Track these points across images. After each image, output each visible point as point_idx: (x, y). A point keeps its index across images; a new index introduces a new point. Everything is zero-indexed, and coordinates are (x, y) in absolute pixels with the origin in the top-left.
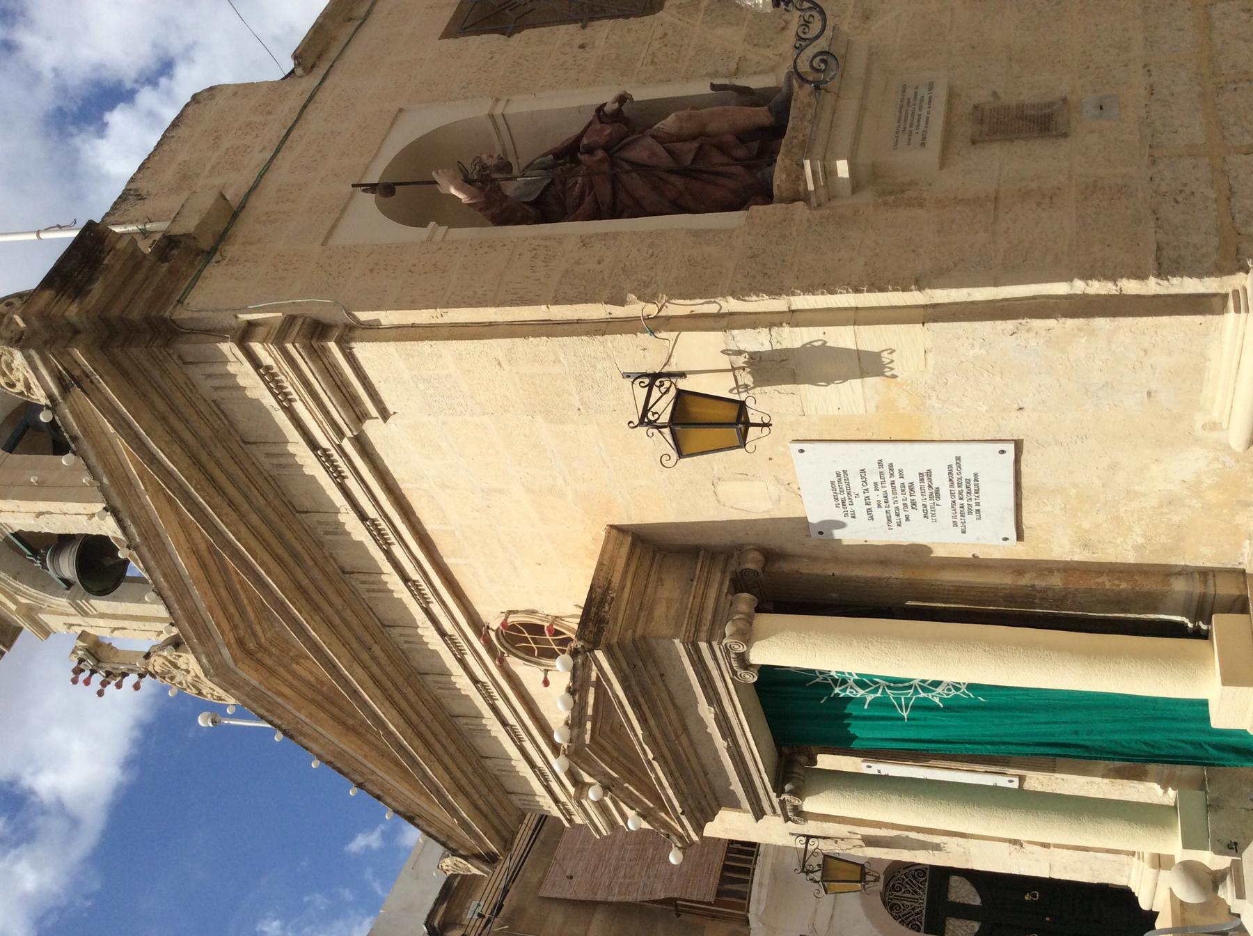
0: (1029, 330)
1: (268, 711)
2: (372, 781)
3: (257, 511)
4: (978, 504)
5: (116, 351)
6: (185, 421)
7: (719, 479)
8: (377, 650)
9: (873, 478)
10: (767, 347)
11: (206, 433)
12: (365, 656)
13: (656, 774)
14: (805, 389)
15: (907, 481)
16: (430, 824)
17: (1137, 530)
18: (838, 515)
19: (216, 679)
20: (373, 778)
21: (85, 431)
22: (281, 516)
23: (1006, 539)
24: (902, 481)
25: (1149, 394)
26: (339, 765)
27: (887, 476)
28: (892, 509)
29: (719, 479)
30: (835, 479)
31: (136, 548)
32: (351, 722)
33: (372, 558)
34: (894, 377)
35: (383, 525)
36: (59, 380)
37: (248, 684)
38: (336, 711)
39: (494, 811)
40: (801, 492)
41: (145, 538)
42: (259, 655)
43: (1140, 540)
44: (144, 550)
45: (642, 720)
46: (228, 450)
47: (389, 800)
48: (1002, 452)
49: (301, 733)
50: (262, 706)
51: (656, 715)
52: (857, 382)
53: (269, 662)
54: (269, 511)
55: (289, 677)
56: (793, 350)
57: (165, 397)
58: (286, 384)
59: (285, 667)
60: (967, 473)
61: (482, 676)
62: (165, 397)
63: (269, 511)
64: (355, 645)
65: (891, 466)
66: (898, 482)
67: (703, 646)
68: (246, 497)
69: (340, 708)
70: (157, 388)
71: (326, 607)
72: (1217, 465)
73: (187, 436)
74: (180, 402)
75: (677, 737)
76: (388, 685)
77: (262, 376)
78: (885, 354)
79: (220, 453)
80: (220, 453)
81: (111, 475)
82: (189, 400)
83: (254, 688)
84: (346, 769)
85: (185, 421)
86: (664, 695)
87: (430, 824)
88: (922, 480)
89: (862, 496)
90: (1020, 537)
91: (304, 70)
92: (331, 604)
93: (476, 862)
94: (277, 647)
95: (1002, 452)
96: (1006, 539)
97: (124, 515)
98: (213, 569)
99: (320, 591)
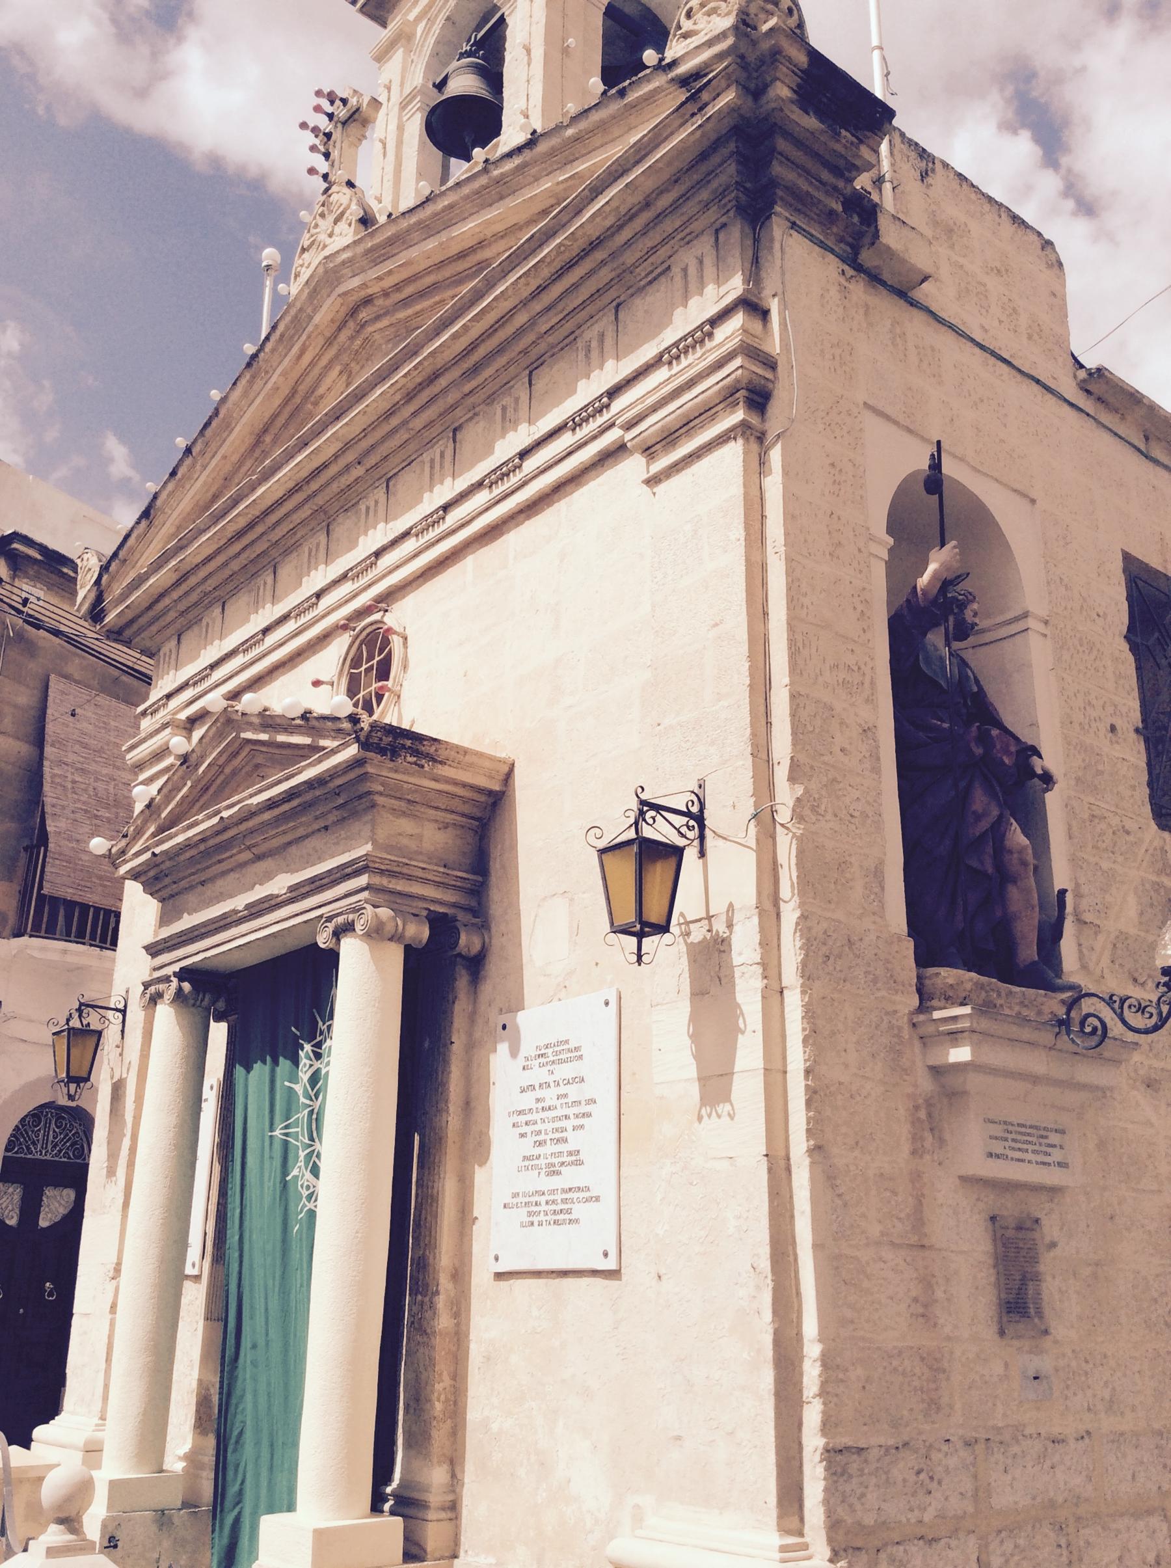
0: (758, 1287)
1: (282, 336)
2: (193, 465)
3: (532, 322)
4: (540, 1224)
5: (732, 146)
6: (644, 232)
7: (572, 900)
8: (359, 471)
9: (573, 1092)
10: (737, 959)
11: (629, 258)
12: (350, 457)
13: (203, 821)
14: (684, 1008)
15: (569, 1134)
16: (140, 538)
18: (528, 1047)
19: (321, 270)
20: (198, 467)
21: (632, 106)
22: (525, 352)
23: (497, 1259)
24: (570, 1128)
25: (679, 1438)
26: (214, 424)
27: (576, 1110)
29: (572, 900)
30: (572, 1045)
31: (485, 170)
32: (268, 439)
33: (472, 465)
34: (700, 1118)
35: (514, 479)
36: (696, 75)
37: (315, 311)
38: (281, 420)
39: (156, 619)
42: (351, 324)
43: (495, 1427)
44: (483, 180)
45: (271, 804)
46: (609, 286)
47: (170, 487)
48: (606, 1255)
49: (253, 377)
50: (287, 328)
51: (278, 821)
52: (692, 1072)
55: (324, 361)
57: (675, 207)
58: (691, 358)
59: (337, 356)
60: (579, 1210)
62: (675, 207)
63: (529, 338)
64: (365, 444)
65: (589, 1115)
66: (568, 1124)
67: (363, 880)
68: (548, 309)
69: (285, 425)
70: (685, 197)
73: (626, 234)
74: (669, 225)
75: (249, 848)
76: (314, 486)
77: (700, 327)
78: (728, 1107)
79: (605, 275)
80: (605, 275)
81: (577, 139)
82: (670, 237)
83: (311, 318)
84: (209, 432)
85: (644, 232)
86: (301, 832)
87: (140, 538)
88: (570, 1154)
89: (550, 1079)
90: (499, 1276)
91: (1084, 381)
92: (415, 414)
93: (93, 595)
94: (362, 347)
95: (606, 1255)
96: (497, 1259)
97: (527, 155)
98: (461, 266)
99: (432, 400)
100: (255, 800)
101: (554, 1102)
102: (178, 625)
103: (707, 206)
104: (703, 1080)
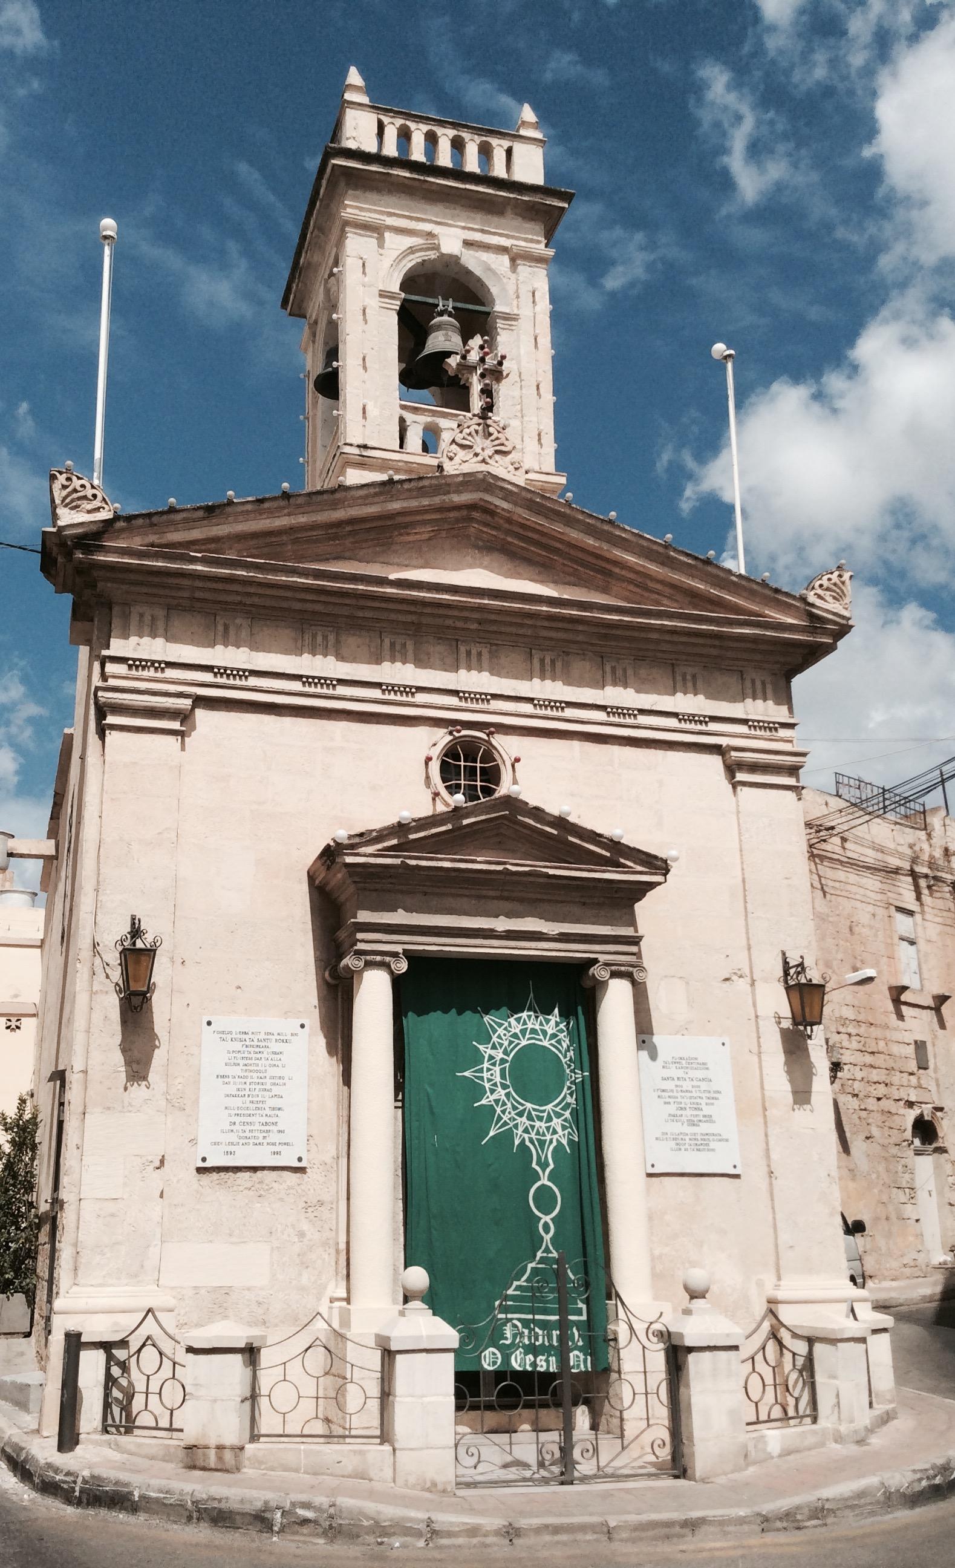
2: (284, 508)
3: (658, 642)
9: (704, 1086)
11: (729, 654)
12: (476, 615)
14: (781, 1058)
15: (703, 1106)
19: (481, 476)
20: (286, 511)
22: (640, 650)
23: (653, 1166)
26: (325, 497)
28: (675, 1094)
29: (687, 983)
32: (348, 528)
33: (580, 685)
35: (629, 721)
37: (458, 492)
40: (679, 1036)
41: (669, 557)
42: (464, 513)
44: (661, 550)
45: (554, 876)
46: (708, 656)
48: (735, 1167)
49: (380, 494)
50: (431, 486)
52: (788, 1087)
53: (452, 515)
54: (651, 647)
55: (428, 517)
56: (808, 1056)
58: (762, 733)
60: (712, 1145)
61: (420, 698)
63: (651, 647)
64: (493, 617)
65: (716, 1099)
66: (703, 1102)
71: (546, 624)
73: (735, 645)
74: (758, 657)
76: (428, 610)
79: (714, 652)
80: (714, 652)
81: (733, 582)
82: (752, 661)
83: (449, 493)
84: (314, 497)
87: (186, 520)
88: (705, 1116)
89: (686, 1076)
90: (650, 1175)
92: (545, 628)
93: (94, 528)
94: (459, 529)
95: (735, 1167)
97: (700, 565)
98: (591, 559)
99: (566, 630)
100: (551, 872)
101: (690, 1088)
102: (175, 602)
103: (777, 663)
104: (795, 1093)
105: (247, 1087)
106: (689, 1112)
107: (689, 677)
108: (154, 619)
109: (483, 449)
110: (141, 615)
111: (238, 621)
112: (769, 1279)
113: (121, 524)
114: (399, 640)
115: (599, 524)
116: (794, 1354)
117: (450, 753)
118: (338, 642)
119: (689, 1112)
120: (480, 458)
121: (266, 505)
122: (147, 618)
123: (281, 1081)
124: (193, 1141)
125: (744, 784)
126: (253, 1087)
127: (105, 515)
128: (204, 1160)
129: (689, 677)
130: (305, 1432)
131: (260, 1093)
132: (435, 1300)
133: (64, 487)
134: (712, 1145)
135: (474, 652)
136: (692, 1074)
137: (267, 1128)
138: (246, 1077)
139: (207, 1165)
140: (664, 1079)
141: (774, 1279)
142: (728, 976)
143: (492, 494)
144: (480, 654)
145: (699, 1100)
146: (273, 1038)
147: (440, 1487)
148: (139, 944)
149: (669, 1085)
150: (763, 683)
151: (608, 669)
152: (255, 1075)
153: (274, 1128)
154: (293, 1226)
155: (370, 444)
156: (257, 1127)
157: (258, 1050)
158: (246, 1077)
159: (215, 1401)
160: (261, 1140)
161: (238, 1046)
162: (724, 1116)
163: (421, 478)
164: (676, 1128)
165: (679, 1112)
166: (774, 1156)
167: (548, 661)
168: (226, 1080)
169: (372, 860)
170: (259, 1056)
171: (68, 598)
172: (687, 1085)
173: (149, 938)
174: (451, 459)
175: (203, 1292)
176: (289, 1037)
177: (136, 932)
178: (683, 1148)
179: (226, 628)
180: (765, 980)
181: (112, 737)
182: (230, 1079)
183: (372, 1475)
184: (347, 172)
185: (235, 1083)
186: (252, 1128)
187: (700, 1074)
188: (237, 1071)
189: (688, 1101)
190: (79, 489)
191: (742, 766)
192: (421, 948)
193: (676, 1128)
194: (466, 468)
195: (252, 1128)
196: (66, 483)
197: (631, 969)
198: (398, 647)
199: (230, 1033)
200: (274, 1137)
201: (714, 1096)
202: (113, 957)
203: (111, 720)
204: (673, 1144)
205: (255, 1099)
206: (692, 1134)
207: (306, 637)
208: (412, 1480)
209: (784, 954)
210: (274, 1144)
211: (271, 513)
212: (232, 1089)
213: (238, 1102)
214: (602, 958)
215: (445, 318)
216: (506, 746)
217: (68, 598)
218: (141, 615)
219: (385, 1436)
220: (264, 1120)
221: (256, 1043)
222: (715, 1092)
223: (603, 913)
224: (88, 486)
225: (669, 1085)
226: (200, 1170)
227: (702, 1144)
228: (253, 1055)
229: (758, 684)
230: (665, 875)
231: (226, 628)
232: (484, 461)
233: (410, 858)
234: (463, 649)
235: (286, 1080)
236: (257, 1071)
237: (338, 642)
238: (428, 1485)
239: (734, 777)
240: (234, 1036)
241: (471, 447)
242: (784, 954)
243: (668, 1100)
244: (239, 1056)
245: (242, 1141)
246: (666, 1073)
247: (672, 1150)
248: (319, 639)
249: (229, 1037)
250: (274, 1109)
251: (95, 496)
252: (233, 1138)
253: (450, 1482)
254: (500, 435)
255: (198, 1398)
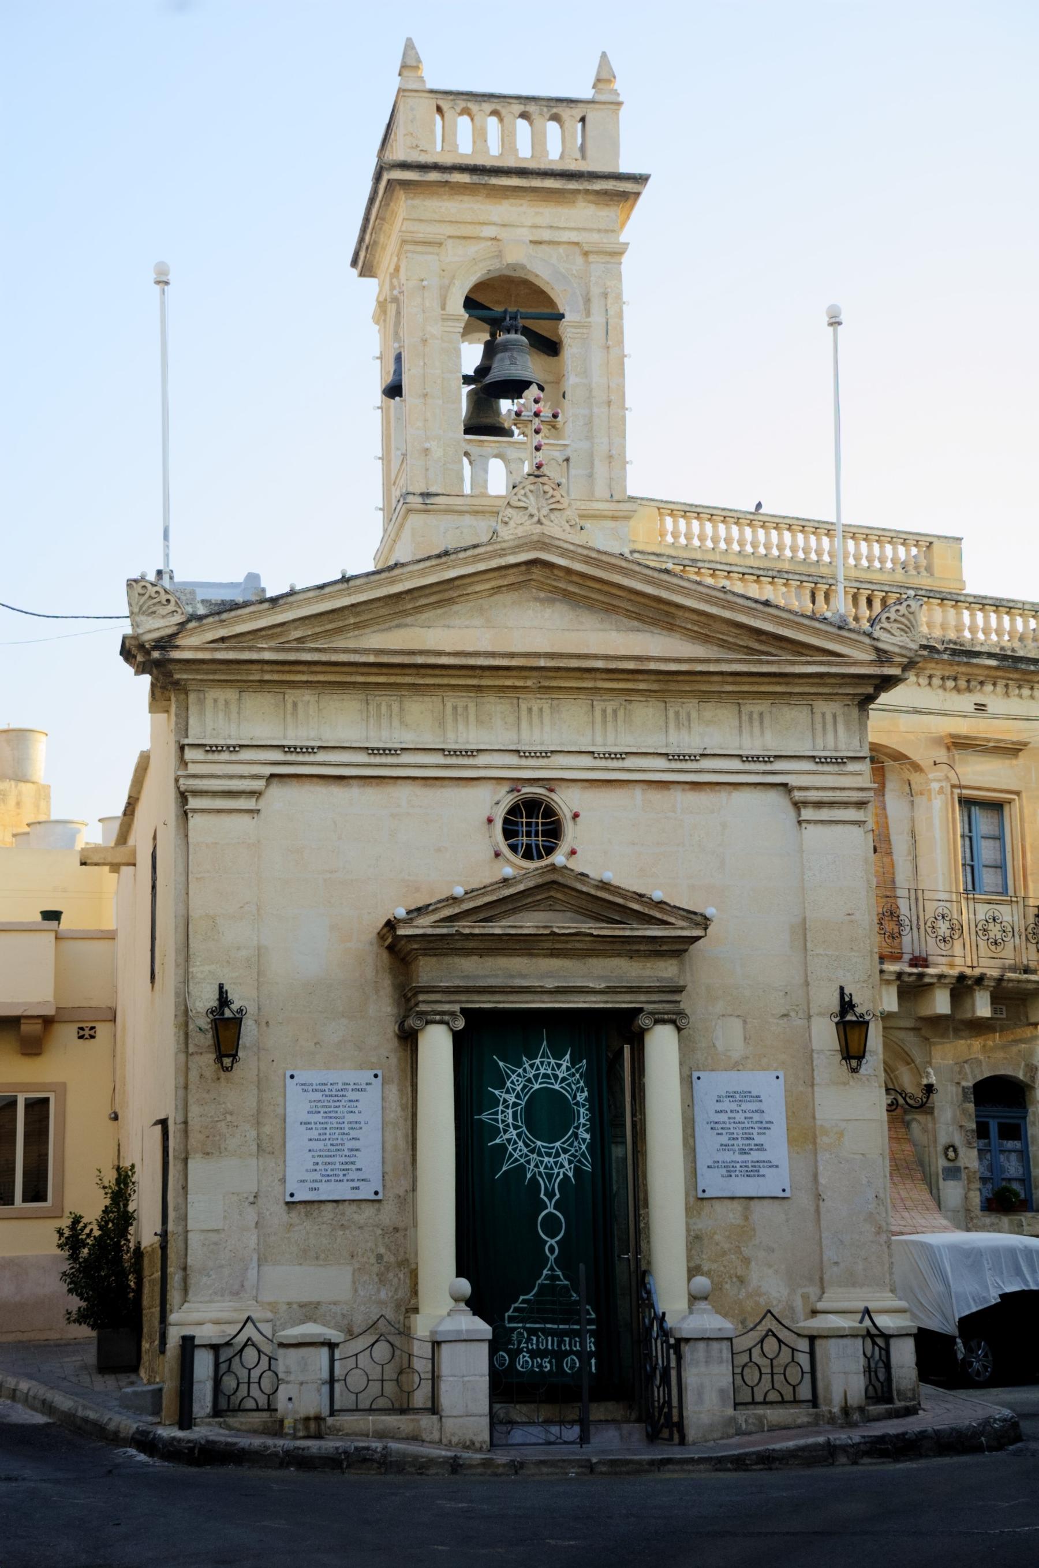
4: (737, 1176)
9: (756, 1117)
15: (755, 1136)
17: (714, 1266)
28: (728, 1125)
29: (745, 1022)
47: (311, 594)
48: (784, 1190)
60: (762, 1171)
66: (755, 1132)
72: (775, 1303)
88: (756, 1145)
93: (169, 631)
95: (784, 1190)
97: (760, 607)
100: (595, 933)
101: (743, 1120)
105: (328, 1131)
106: (740, 1142)
107: (755, 716)
108: (227, 703)
109: (539, 510)
110: (215, 701)
111: (307, 698)
112: (813, 1291)
113: (192, 625)
114: (461, 703)
115: (656, 574)
116: (793, 1350)
117: (514, 811)
118: (402, 710)
119: (740, 1142)
120: (535, 519)
121: (327, 590)
122: (221, 703)
123: (358, 1126)
124: (283, 1180)
125: (808, 822)
126: (333, 1131)
127: (178, 618)
128: (292, 1195)
129: (755, 716)
130: (374, 1407)
131: (340, 1137)
132: (476, 1304)
133: (141, 595)
134: (762, 1171)
135: (535, 709)
136: (744, 1106)
137: (347, 1167)
138: (327, 1123)
139: (295, 1199)
140: (717, 1112)
141: (818, 1292)
142: (785, 1012)
143: (549, 551)
144: (541, 710)
145: (751, 1131)
146: (350, 1087)
147: (478, 1445)
148: (228, 1014)
149: (722, 1118)
150: (835, 716)
151: (671, 714)
152: (334, 1121)
153: (353, 1167)
154: (372, 1251)
155: (433, 490)
156: (337, 1166)
157: (336, 1099)
158: (327, 1123)
159: (302, 1384)
160: (341, 1177)
161: (318, 1096)
162: (776, 1145)
163: (475, 546)
164: (728, 1156)
165: (731, 1142)
166: (822, 1180)
167: (609, 711)
168: (309, 1126)
169: (429, 931)
170: (337, 1104)
171: (147, 679)
172: (740, 1117)
173: (235, 1007)
174: (506, 523)
175: (295, 1306)
176: (364, 1086)
177: (224, 1000)
178: (733, 1174)
179: (295, 705)
180: (820, 1014)
181: (194, 821)
182: (313, 1126)
183: (424, 1436)
184: (405, 184)
185: (317, 1129)
186: (333, 1167)
187: (753, 1106)
188: (318, 1118)
189: (741, 1131)
190: (154, 595)
191: (806, 803)
192: (477, 1006)
193: (728, 1156)
194: (520, 532)
195: (333, 1167)
196: (142, 591)
197: (674, 1017)
198: (460, 710)
199: (312, 1085)
200: (352, 1175)
201: (765, 1127)
202: (204, 1022)
203: (193, 803)
204: (724, 1171)
205: (335, 1142)
206: (743, 1162)
207: (371, 708)
208: (455, 1440)
209: (842, 989)
210: (353, 1180)
211: (331, 596)
212: (314, 1134)
213: (320, 1145)
214: (645, 1006)
215: (513, 336)
216: (565, 801)
217: (147, 679)
218: (215, 701)
219: (434, 1409)
220: (343, 1159)
221: (334, 1093)
222: (767, 1122)
223: (649, 965)
224: (162, 592)
225: (722, 1118)
226: (287, 1203)
227: (753, 1171)
228: (333, 1104)
229: (829, 718)
230: (706, 929)
231: (295, 705)
232: (539, 522)
233: (464, 927)
234: (524, 706)
235: (362, 1125)
236: (336, 1118)
237: (402, 710)
238: (468, 1443)
239: (799, 815)
240: (314, 1087)
241: (526, 508)
242: (842, 989)
243: (720, 1131)
244: (320, 1104)
245: (324, 1179)
246: (720, 1106)
247: (722, 1176)
248: (384, 709)
249: (310, 1088)
250: (352, 1150)
251: (168, 601)
252: (317, 1176)
253: (485, 1442)
254: (555, 493)
255: (288, 1382)
